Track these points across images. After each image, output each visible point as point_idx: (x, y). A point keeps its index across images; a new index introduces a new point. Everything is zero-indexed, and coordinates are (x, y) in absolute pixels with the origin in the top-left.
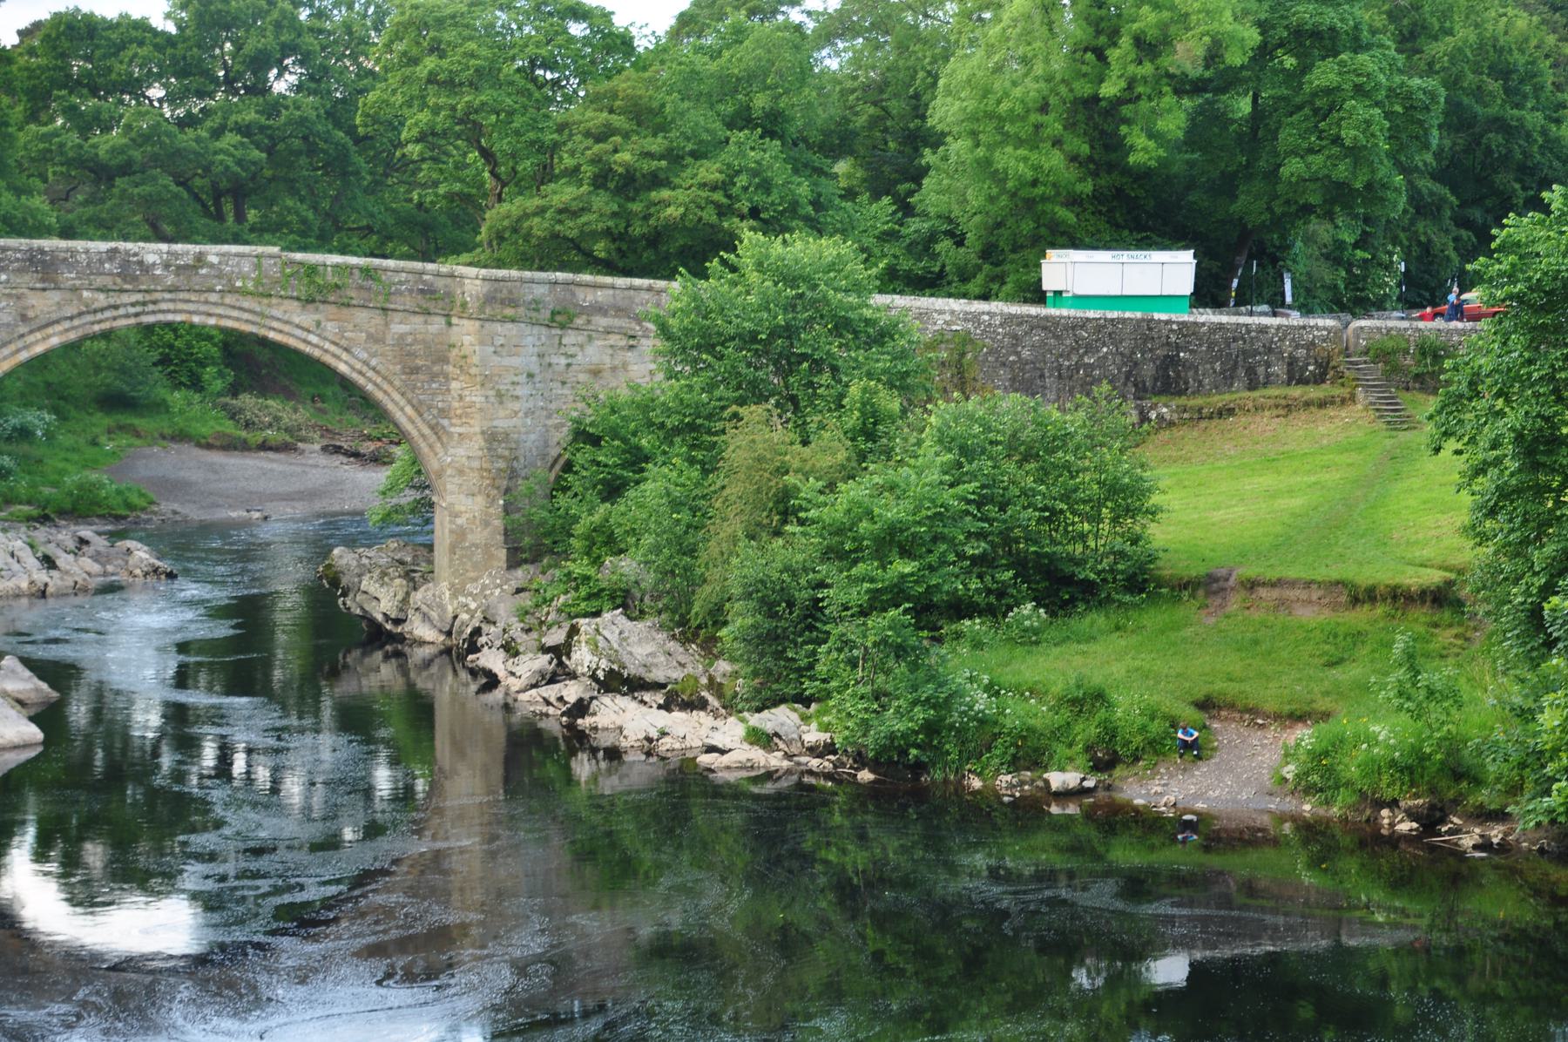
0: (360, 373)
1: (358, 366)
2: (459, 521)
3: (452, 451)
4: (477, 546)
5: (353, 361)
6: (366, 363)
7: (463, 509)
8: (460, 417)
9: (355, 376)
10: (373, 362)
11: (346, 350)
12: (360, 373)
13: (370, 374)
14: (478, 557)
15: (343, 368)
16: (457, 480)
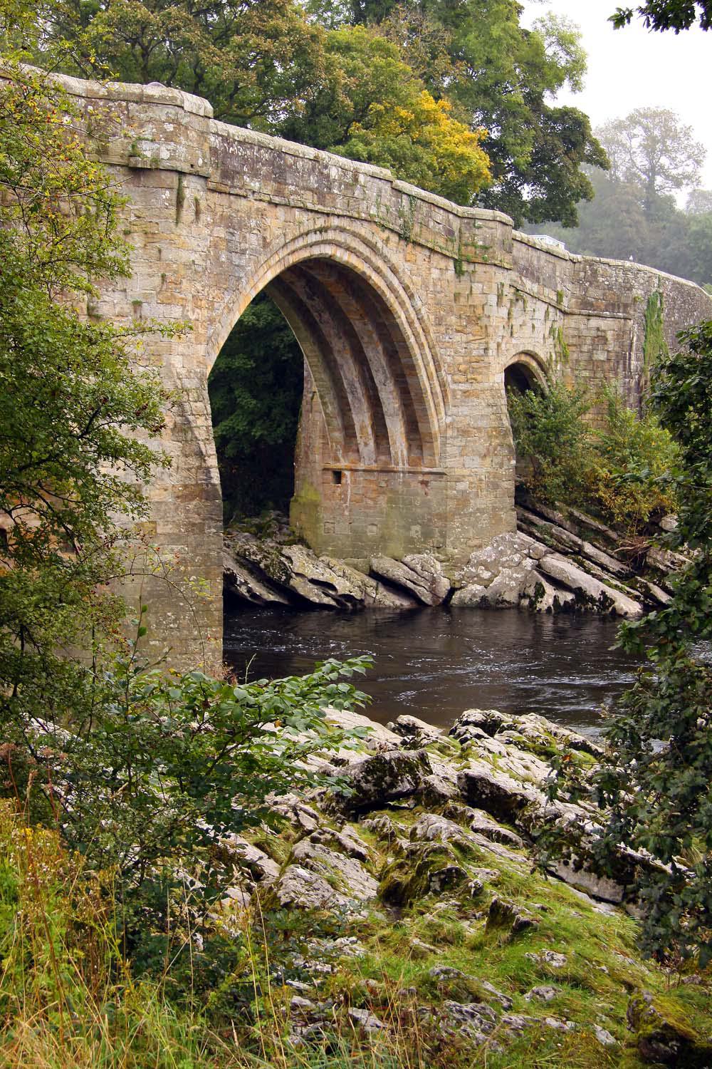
0: (411, 324)
1: (413, 316)
2: (461, 486)
3: (452, 410)
4: (482, 511)
5: (411, 310)
6: (418, 312)
7: (466, 472)
8: (465, 373)
9: (406, 326)
10: (423, 311)
11: (411, 297)
12: (411, 324)
13: (417, 324)
14: (484, 521)
15: (402, 318)
16: (458, 442)
